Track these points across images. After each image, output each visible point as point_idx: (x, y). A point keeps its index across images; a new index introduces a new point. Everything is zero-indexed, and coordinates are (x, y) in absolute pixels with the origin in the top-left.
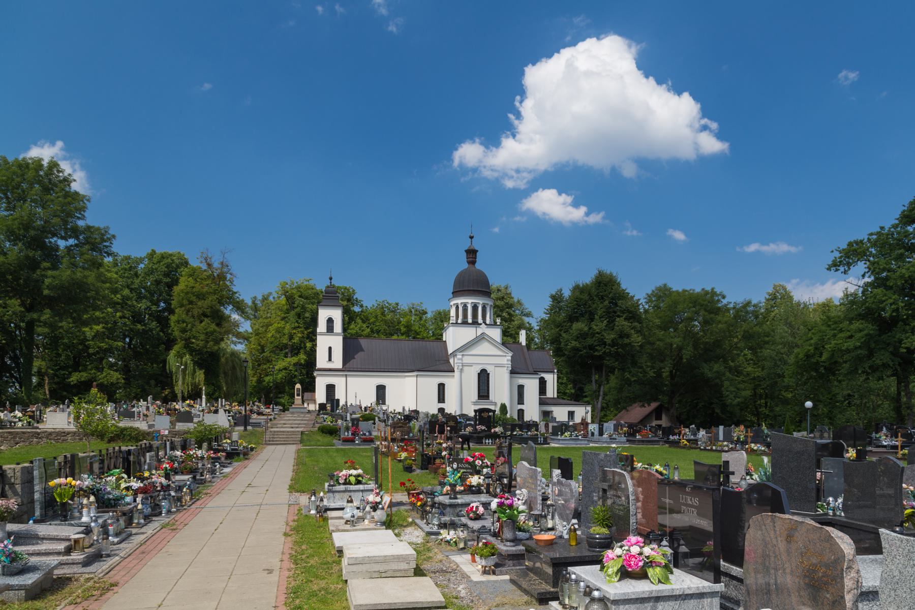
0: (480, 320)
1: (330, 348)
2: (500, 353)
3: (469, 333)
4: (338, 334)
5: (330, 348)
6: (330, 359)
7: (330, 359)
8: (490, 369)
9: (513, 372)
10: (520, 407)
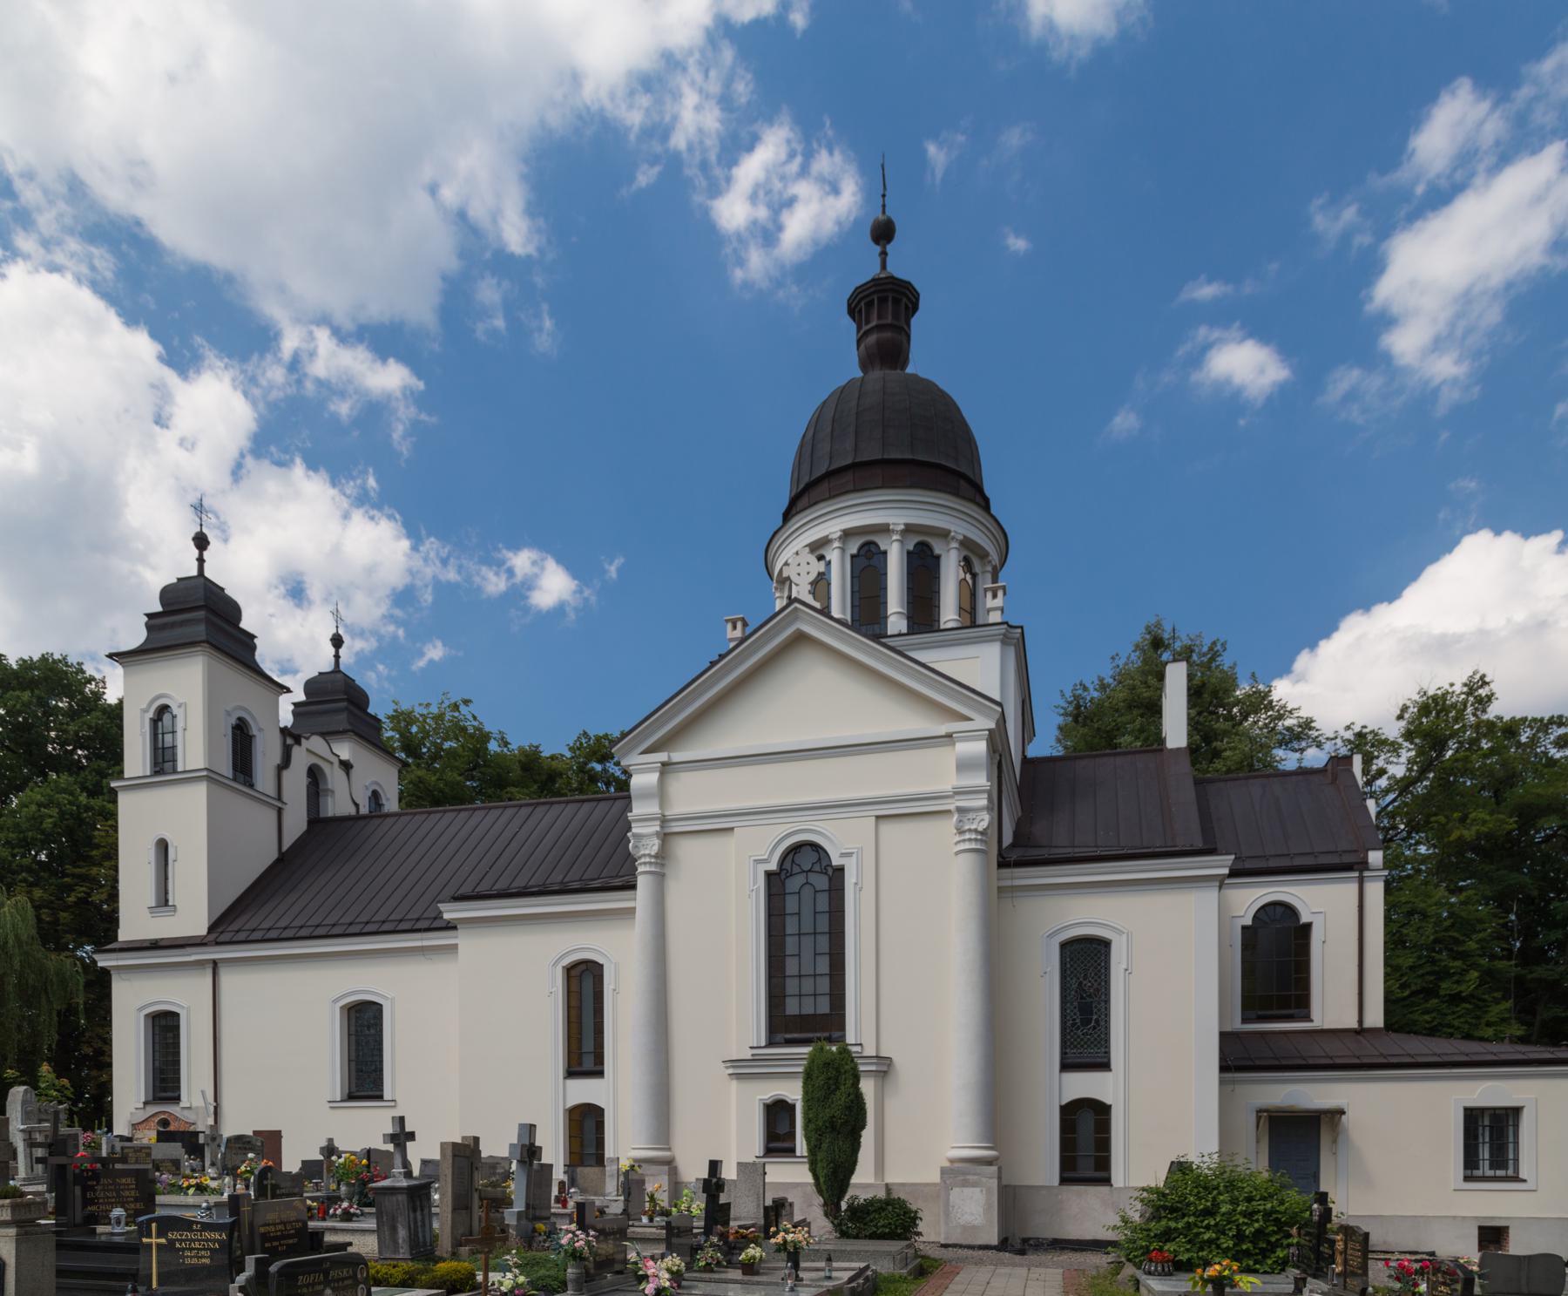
1: (163, 846)
2: (915, 723)
5: (163, 846)
8: (843, 840)
10: (1083, 1085)
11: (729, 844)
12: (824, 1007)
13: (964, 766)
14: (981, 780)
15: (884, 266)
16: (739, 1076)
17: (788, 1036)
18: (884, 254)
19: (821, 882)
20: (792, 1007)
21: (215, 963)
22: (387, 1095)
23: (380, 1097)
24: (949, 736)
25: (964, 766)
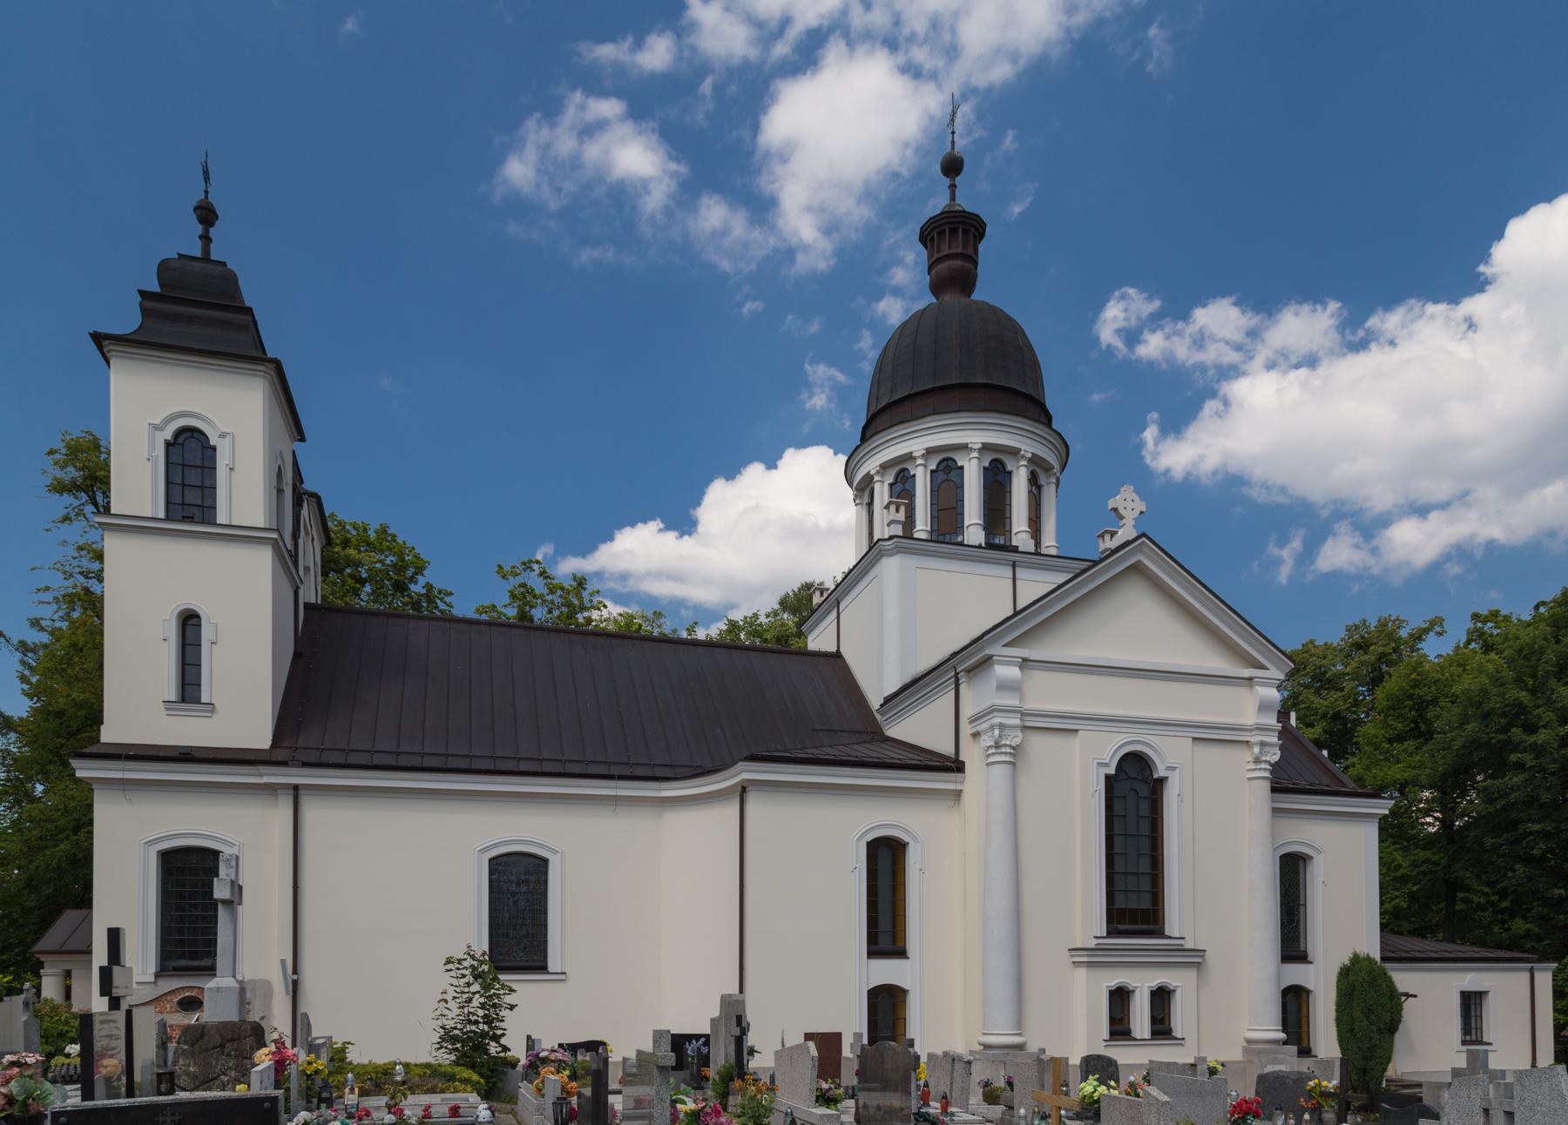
0: (1020, 533)
1: (189, 622)
2: (1215, 662)
3: (970, 597)
4: (241, 536)
5: (189, 622)
6: (189, 689)
7: (189, 689)
8: (1169, 754)
9: (1282, 784)
11: (1077, 742)
12: (1145, 904)
13: (1263, 707)
14: (1272, 720)
15: (953, 198)
16: (1089, 965)
17: (1121, 927)
18: (953, 187)
19: (1144, 790)
20: (1119, 905)
21: (296, 788)
22: (553, 964)
23: (543, 968)
24: (1250, 679)
25: (1263, 707)
